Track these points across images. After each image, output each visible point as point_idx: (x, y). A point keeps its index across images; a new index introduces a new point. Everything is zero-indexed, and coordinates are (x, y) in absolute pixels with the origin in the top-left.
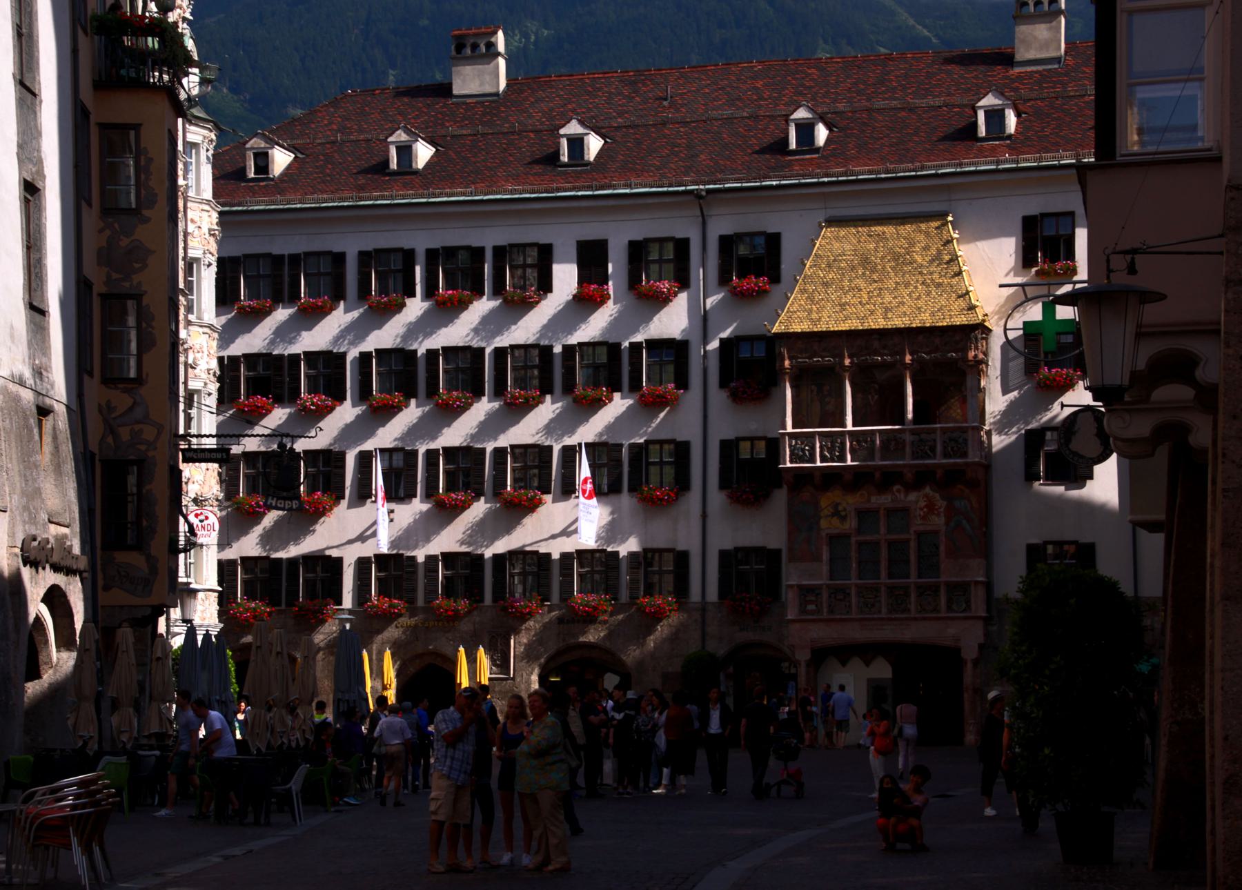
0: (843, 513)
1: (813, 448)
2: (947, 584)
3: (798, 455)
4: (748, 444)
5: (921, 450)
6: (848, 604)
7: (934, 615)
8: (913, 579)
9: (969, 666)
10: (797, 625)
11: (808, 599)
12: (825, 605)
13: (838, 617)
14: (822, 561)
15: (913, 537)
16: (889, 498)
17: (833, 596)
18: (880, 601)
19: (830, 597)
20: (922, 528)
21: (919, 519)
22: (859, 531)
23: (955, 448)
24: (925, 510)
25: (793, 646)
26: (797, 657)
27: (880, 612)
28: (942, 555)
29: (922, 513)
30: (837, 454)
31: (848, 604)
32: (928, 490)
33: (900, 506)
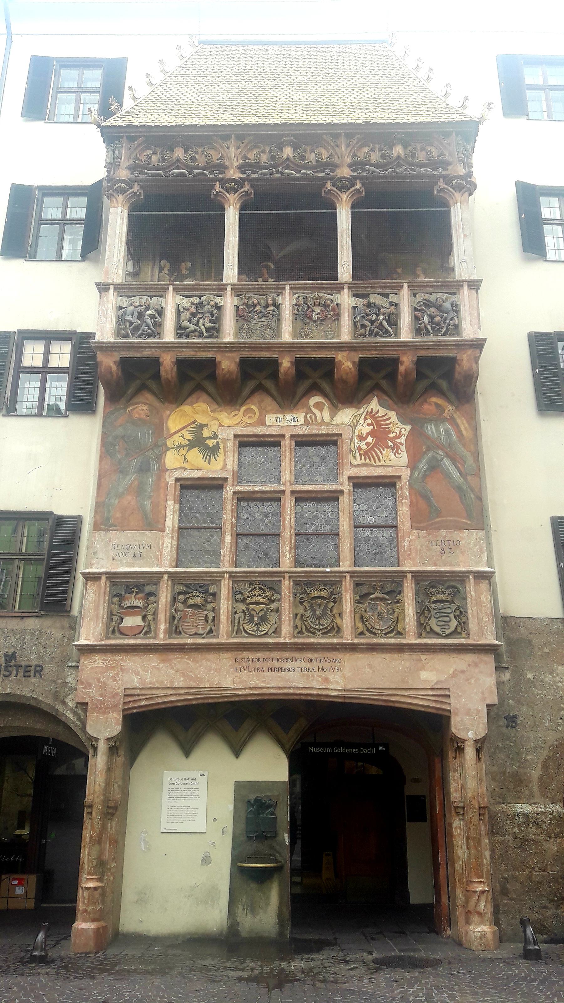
0: (211, 443)
1: (161, 312)
2: (418, 576)
3: (131, 324)
4: (40, 347)
5: (372, 322)
6: (211, 615)
7: (392, 641)
8: (346, 565)
9: (470, 752)
10: (98, 660)
11: (126, 604)
12: (162, 617)
13: (190, 641)
14: (163, 530)
15: (347, 487)
16: (301, 417)
17: (181, 597)
18: (277, 611)
19: (174, 600)
20: (363, 472)
21: (358, 454)
22: (239, 477)
23: (438, 319)
24: (370, 439)
25: (84, 705)
26: (90, 731)
27: (277, 632)
28: (405, 524)
29: (363, 446)
30: (208, 325)
31: (211, 615)
32: (374, 405)
33: (323, 432)
